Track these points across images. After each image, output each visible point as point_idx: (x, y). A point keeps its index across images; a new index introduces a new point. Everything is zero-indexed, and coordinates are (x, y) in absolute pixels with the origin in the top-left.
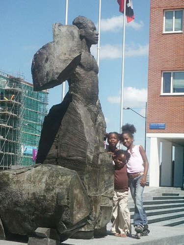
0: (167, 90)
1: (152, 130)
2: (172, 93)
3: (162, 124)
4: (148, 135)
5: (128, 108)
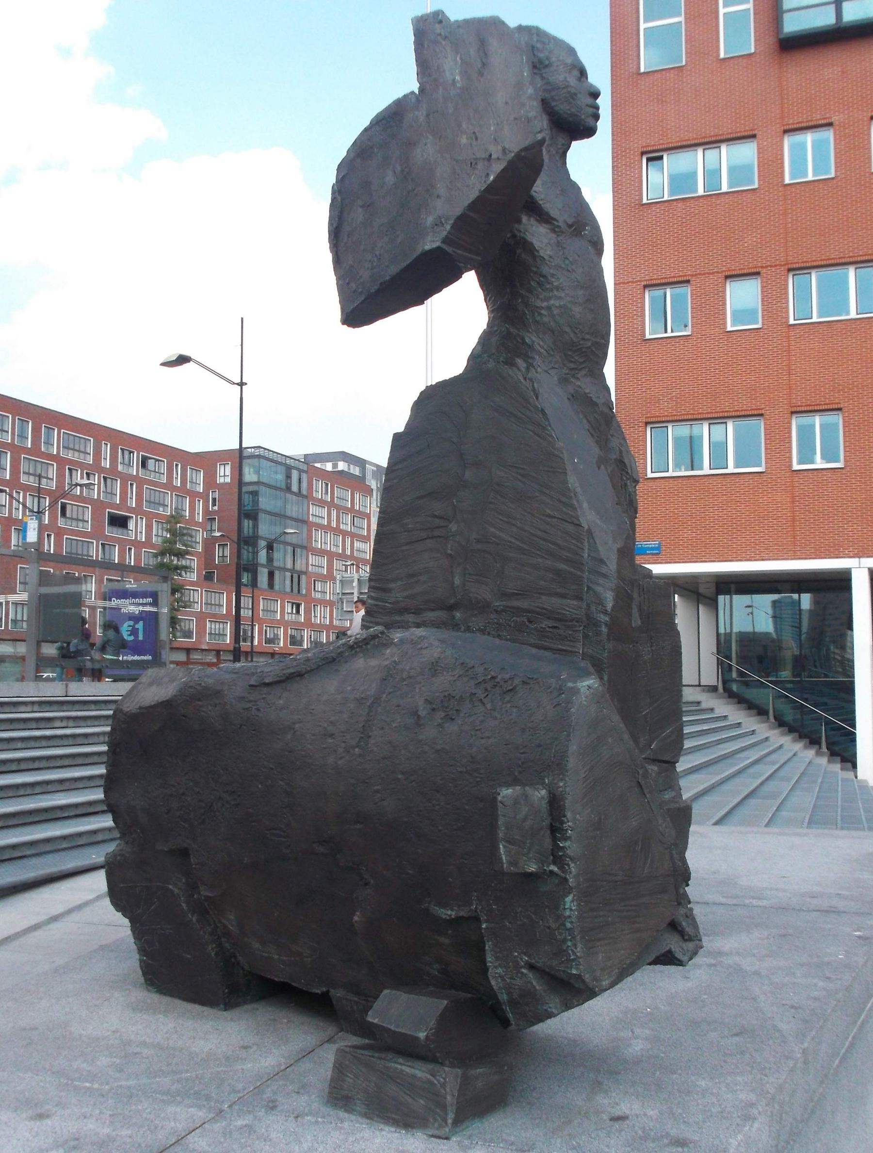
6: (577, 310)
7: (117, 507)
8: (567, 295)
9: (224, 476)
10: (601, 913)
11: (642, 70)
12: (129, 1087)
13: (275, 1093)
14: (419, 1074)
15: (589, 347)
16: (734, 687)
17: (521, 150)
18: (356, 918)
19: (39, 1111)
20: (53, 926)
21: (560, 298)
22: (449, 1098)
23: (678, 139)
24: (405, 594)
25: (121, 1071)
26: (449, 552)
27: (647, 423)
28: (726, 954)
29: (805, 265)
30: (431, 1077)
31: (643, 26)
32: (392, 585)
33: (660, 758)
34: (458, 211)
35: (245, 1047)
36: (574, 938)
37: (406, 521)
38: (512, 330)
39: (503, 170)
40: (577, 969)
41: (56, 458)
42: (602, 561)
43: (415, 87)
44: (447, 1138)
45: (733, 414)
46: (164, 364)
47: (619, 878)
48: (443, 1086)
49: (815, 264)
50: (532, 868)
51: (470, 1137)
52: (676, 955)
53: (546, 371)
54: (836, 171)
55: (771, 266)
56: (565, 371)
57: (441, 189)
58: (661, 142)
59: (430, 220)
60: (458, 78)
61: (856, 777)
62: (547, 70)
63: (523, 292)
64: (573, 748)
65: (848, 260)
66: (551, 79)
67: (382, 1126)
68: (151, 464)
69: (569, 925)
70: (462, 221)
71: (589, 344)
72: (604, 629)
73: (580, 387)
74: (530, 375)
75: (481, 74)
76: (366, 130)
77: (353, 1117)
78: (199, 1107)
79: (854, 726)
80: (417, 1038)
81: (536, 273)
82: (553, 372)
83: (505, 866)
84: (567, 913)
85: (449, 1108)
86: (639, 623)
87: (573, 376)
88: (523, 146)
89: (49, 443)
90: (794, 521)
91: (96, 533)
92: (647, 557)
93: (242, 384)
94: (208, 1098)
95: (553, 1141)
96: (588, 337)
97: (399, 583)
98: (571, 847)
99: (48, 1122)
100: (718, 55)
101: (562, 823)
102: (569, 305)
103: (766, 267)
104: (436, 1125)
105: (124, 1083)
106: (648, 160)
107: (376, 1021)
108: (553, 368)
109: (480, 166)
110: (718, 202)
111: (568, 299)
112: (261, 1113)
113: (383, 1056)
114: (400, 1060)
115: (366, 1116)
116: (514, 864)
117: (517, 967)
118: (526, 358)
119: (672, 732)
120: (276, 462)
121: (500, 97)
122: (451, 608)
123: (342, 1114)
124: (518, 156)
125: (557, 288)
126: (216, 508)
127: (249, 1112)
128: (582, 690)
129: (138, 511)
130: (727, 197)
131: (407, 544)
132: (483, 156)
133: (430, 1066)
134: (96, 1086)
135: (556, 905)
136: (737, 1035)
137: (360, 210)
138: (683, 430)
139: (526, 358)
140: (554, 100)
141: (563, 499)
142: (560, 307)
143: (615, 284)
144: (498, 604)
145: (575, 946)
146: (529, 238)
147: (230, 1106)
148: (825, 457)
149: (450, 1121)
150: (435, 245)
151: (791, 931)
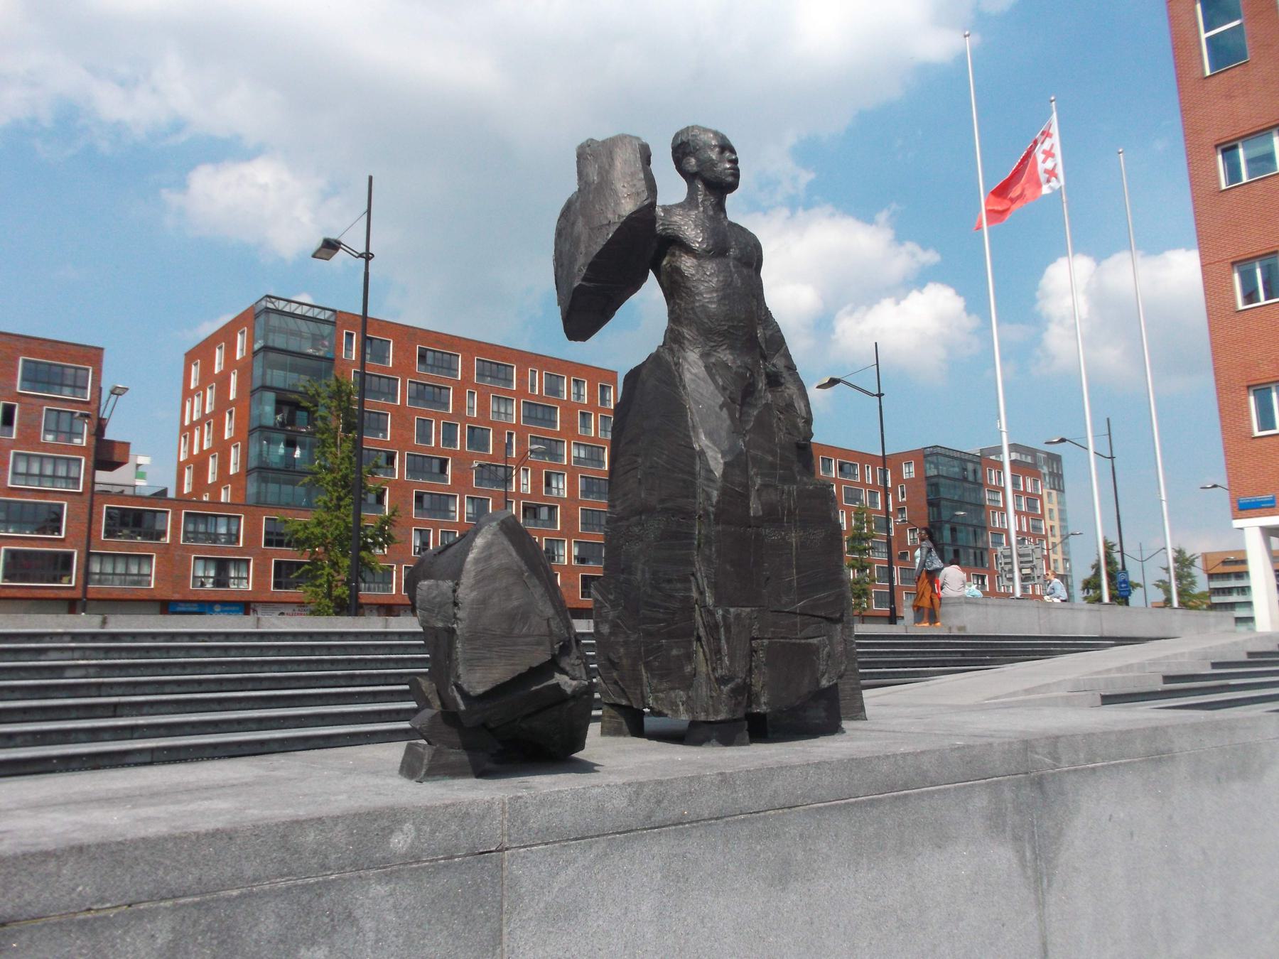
1: (1243, 512)
3: (1269, 496)
4: (1237, 523)
5: (1215, 486)
9: (909, 472)
11: (1208, 73)
15: (726, 330)
17: (632, 214)
23: (1251, 127)
24: (622, 507)
27: (1248, 387)
31: (1204, 36)
33: (810, 613)
39: (618, 230)
42: (711, 471)
43: (575, 188)
47: (498, 633)
50: (440, 625)
53: (692, 351)
56: (707, 348)
57: (582, 249)
58: (1234, 132)
59: (577, 268)
60: (595, 178)
63: (678, 301)
64: (471, 556)
66: (701, 157)
70: (592, 266)
71: (726, 328)
72: (712, 517)
75: (608, 172)
76: (559, 220)
82: (697, 350)
86: (761, 513)
87: (715, 351)
92: (1262, 510)
93: (880, 395)
96: (723, 323)
98: (460, 614)
102: (706, 304)
106: (1224, 151)
109: (604, 230)
118: (681, 344)
122: (641, 513)
132: (606, 222)
140: (703, 170)
142: (700, 306)
143: (1203, 266)
144: (659, 507)
149: (423, 773)
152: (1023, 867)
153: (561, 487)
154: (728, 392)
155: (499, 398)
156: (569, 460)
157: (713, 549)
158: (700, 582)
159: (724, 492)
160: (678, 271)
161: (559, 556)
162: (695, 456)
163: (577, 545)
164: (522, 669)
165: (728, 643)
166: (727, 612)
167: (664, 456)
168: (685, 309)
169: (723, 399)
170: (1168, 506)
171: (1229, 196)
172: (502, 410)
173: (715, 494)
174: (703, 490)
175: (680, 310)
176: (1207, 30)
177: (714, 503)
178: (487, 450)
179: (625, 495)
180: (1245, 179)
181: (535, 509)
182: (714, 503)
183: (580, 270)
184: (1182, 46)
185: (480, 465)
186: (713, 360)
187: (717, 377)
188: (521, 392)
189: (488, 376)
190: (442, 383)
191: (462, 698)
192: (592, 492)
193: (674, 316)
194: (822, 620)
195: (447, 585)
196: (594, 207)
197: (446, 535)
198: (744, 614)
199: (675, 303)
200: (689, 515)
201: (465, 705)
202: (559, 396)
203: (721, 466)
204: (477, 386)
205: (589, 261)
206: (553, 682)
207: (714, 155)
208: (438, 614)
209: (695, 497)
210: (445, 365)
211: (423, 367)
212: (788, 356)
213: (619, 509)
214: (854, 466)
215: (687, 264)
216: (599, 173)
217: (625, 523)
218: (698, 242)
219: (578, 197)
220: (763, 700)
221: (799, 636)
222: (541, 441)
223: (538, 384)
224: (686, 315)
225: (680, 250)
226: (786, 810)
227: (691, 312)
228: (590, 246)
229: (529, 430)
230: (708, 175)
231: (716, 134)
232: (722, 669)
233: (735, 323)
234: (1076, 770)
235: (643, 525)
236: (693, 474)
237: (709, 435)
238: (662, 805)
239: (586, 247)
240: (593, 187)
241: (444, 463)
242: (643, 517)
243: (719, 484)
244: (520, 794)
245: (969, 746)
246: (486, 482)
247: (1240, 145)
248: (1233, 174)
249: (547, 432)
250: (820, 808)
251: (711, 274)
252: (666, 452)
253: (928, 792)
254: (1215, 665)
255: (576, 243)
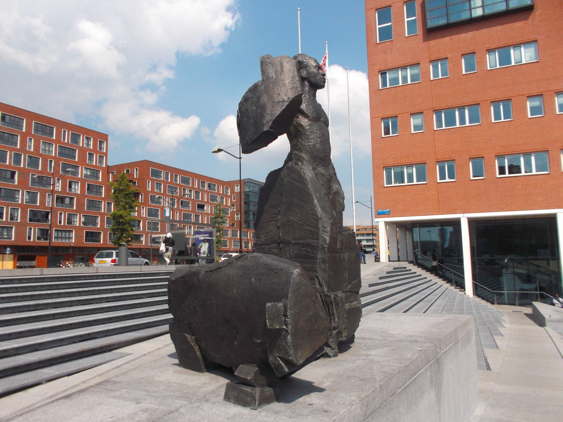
0: (389, 182)
1: (379, 216)
2: (393, 185)
4: (377, 220)
6: (318, 145)
7: (200, 201)
8: (314, 141)
10: (300, 341)
11: (378, 42)
12: (166, 395)
13: (209, 397)
14: (249, 390)
15: (322, 157)
16: (420, 262)
17: (295, 97)
18: (235, 343)
19: (138, 401)
20: (166, 348)
21: (312, 142)
22: (257, 397)
24: (265, 239)
25: (166, 390)
26: (278, 225)
28: (371, 356)
29: (439, 108)
30: (252, 391)
31: (378, 27)
32: (261, 236)
34: (274, 118)
35: (205, 384)
36: (290, 348)
37: (265, 215)
38: (297, 153)
40: (291, 358)
41: (179, 185)
42: (325, 227)
43: (261, 79)
44: (256, 410)
45: (415, 163)
46: (212, 152)
47: (306, 330)
48: (255, 394)
49: (443, 108)
50: (278, 327)
51: (263, 410)
52: (329, 354)
54: (450, 75)
55: (427, 109)
59: (265, 122)
61: (465, 294)
62: (307, 68)
64: (290, 290)
65: (455, 106)
67: (238, 406)
68: (211, 186)
69: (289, 344)
71: (323, 156)
72: (326, 249)
73: (320, 170)
74: (302, 168)
75: (281, 74)
76: (246, 93)
77: (230, 404)
78: (186, 401)
79: (464, 275)
80: (247, 379)
81: (304, 134)
83: (268, 326)
84: (288, 341)
85: (257, 401)
88: (295, 96)
89: (176, 180)
90: (439, 201)
91: (193, 212)
93: (240, 158)
94: (189, 398)
95: (287, 411)
96: (322, 154)
97: (263, 235)
99: (140, 404)
100: (405, 36)
101: (287, 313)
103: (425, 110)
104: (253, 405)
105: (165, 394)
106: (381, 74)
107: (236, 374)
108: (310, 165)
109: (281, 103)
110: (407, 87)
111: (315, 142)
112: (203, 402)
113: (239, 385)
114: (244, 386)
115: (234, 403)
116: (272, 326)
117: (276, 357)
118: (302, 162)
119: (357, 282)
120: (256, 184)
121: (287, 82)
122: (279, 244)
123: (227, 403)
124: (293, 99)
125: (311, 139)
126: (235, 201)
127: (200, 402)
128: (294, 273)
129: (207, 202)
130: (410, 85)
131: (266, 222)
132: (282, 100)
133: (252, 388)
134: (157, 395)
135: (286, 338)
136: (361, 381)
137: (245, 118)
138: (399, 170)
139: (302, 162)
141: (312, 207)
145: (291, 350)
146: (301, 123)
147: (195, 401)
148: (449, 177)
149: (257, 404)
150: (267, 129)
151: (397, 348)
152: (436, 397)
153: (77, 189)
154: (325, 187)
155: (45, 142)
156: (82, 176)
157: (327, 265)
158: (321, 281)
159: (332, 238)
160: (301, 125)
161: (74, 221)
162: (317, 219)
163: (84, 217)
164: (317, 348)
165: (337, 311)
166: (337, 296)
167: (297, 217)
168: (304, 145)
169: (325, 192)
170: (355, 212)
171: (382, 92)
172: (47, 149)
173: (328, 238)
174: (321, 236)
175: (302, 145)
176: (379, 24)
177: (328, 243)
178: (38, 168)
179: (267, 233)
180: (388, 87)
181: (62, 199)
182: (328, 243)
183: (268, 122)
184: (370, 29)
185: (38, 177)
186: (317, 172)
187: (320, 180)
188: (58, 141)
189: (40, 131)
190: (14, 133)
191: (286, 365)
192: (93, 191)
193: (294, 146)
194: (355, 293)
195: (280, 304)
196: (274, 91)
197: (13, 210)
198: (343, 297)
199: (298, 141)
200: (314, 248)
201: (288, 369)
202: (78, 144)
203: (330, 226)
204: (33, 136)
205: (274, 119)
206: (324, 352)
207: (315, 70)
208: (277, 321)
209: (318, 239)
210: (16, 123)
211: (3, 123)
212: (334, 169)
213: (263, 239)
214: (215, 185)
215: (304, 122)
216: (275, 74)
217: (267, 247)
218: (311, 113)
219: (262, 84)
220: (344, 335)
221: (348, 302)
222: (71, 166)
223: (67, 139)
224: (305, 149)
225: (301, 115)
226: (393, 396)
227: (307, 147)
228: (273, 111)
229: (61, 160)
230: (313, 80)
231: (316, 61)
232: (334, 323)
233: (326, 154)
234: (444, 353)
235: (281, 249)
236: (318, 229)
237: (323, 208)
238: (368, 407)
239: (271, 111)
240: (272, 80)
241: (14, 173)
242: (281, 245)
243: (329, 234)
244: (334, 418)
245: (426, 350)
246: (36, 184)
247: (387, 73)
248: (384, 84)
249: (70, 162)
250: (400, 391)
251: (317, 130)
252: (299, 215)
253: (419, 374)
254: (380, 278)
255: (263, 108)
